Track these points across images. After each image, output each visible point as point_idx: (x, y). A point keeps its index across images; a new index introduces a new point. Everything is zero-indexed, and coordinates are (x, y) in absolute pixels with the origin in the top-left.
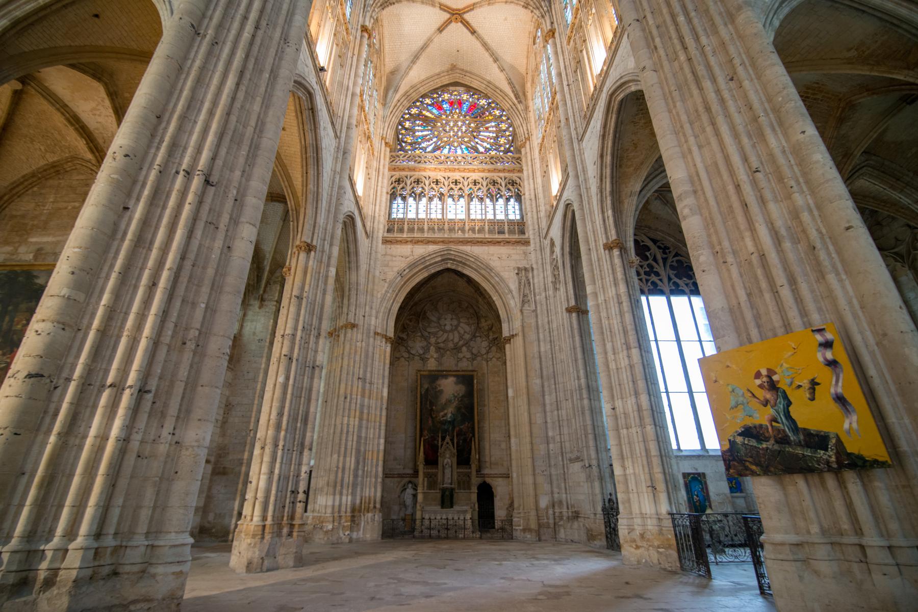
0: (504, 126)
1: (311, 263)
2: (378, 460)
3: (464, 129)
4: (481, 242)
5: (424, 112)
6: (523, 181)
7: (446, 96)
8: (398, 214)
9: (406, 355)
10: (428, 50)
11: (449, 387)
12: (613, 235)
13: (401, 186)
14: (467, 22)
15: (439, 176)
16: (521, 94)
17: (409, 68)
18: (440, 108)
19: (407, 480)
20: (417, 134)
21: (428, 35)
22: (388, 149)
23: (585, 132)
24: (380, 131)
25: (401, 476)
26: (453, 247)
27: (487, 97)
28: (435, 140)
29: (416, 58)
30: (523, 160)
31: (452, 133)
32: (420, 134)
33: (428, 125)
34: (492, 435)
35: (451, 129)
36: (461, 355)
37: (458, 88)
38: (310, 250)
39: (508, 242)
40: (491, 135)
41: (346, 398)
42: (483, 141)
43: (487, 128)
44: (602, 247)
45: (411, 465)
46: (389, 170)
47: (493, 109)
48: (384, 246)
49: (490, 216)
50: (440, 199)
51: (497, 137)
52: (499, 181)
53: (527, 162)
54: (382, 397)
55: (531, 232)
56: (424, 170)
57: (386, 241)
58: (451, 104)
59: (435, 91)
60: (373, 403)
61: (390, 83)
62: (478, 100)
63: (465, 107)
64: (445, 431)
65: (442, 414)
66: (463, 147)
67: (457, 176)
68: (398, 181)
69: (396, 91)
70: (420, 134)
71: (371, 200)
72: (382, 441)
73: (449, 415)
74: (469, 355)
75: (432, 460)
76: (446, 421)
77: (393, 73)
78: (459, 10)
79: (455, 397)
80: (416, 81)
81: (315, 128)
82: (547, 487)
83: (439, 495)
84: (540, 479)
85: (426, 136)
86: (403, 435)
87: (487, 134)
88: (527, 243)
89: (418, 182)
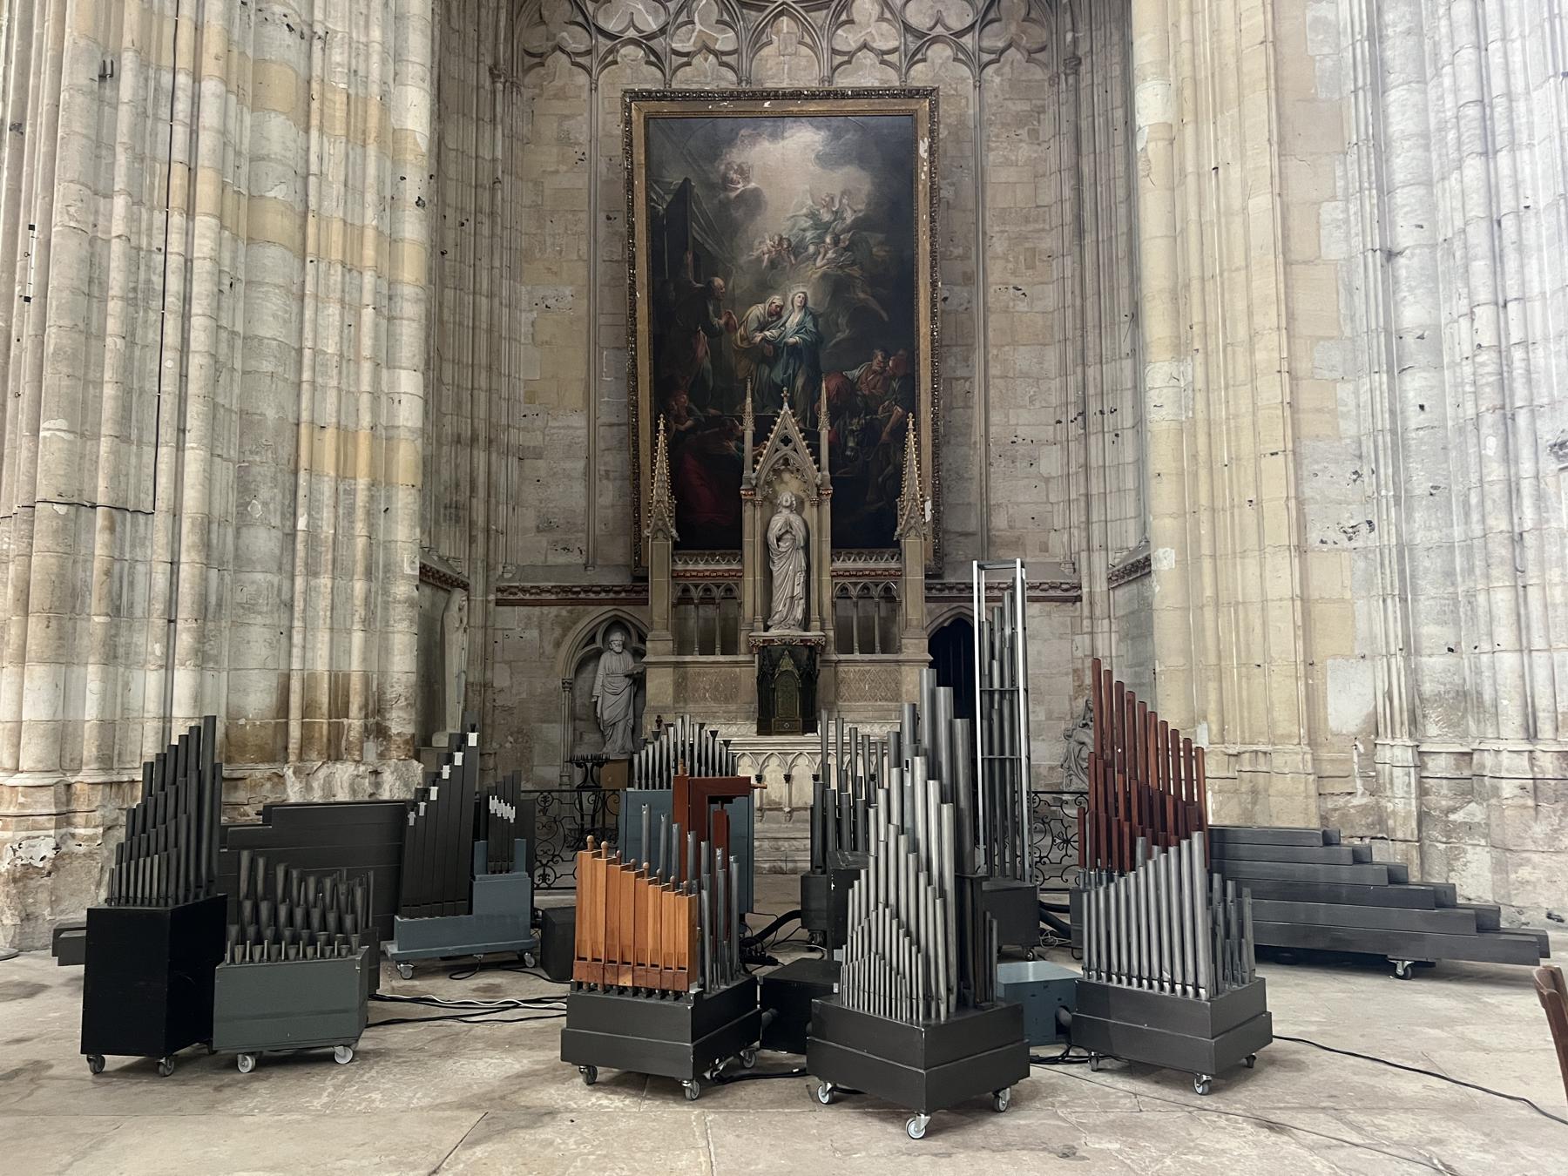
2: (381, 482)
9: (575, 39)
11: (793, 174)
19: (606, 611)
25: (570, 596)
34: (995, 417)
36: (847, 39)
41: (106, 75)
45: (618, 551)
54: (392, 140)
60: (329, 152)
64: (769, 399)
65: (757, 311)
72: (408, 382)
73: (794, 318)
74: (886, 37)
75: (709, 513)
76: (774, 352)
79: (821, 227)
82: (1377, 620)
83: (748, 676)
84: (1334, 575)
86: (579, 421)
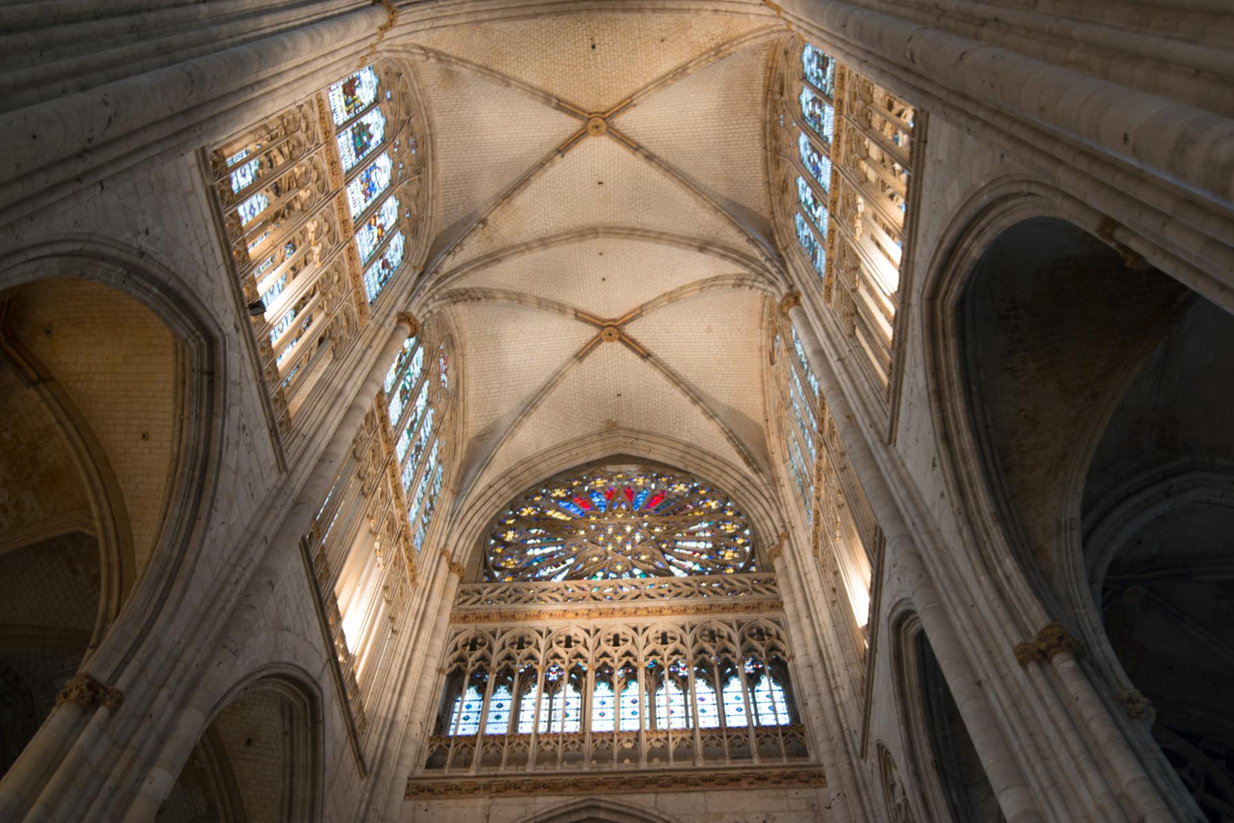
0: (729, 528)
1: (84, 737)
3: (638, 537)
4: (684, 781)
5: (550, 513)
6: (786, 628)
7: (600, 483)
8: (463, 725)
10: (556, 392)
12: (1036, 617)
13: (478, 653)
14: (633, 341)
15: (575, 628)
16: (758, 458)
17: (516, 424)
18: (587, 505)
20: (530, 552)
21: (556, 366)
22: (455, 578)
23: (894, 418)
24: (438, 539)
26: (605, 798)
27: (686, 476)
28: (570, 561)
29: (529, 406)
30: (781, 581)
31: (610, 548)
32: (538, 552)
33: (558, 533)
35: (610, 539)
37: (625, 468)
38: (94, 703)
39: (761, 779)
40: (702, 545)
42: (682, 558)
43: (693, 533)
44: (1013, 662)
46: (453, 619)
47: (704, 498)
48: (409, 804)
49: (709, 720)
50: (577, 686)
51: (716, 549)
52: (725, 630)
53: (789, 585)
55: (823, 747)
56: (538, 615)
57: (416, 790)
58: (610, 495)
59: (574, 472)
61: (477, 454)
62: (669, 484)
63: (641, 499)
66: (637, 571)
67: (619, 625)
68: (473, 644)
69: (485, 465)
70: (538, 552)
71: (391, 682)
77: (481, 437)
78: (615, 320)
80: (530, 452)
81: (211, 414)
85: (551, 555)
87: (693, 545)
88: (815, 778)
89: (521, 643)
